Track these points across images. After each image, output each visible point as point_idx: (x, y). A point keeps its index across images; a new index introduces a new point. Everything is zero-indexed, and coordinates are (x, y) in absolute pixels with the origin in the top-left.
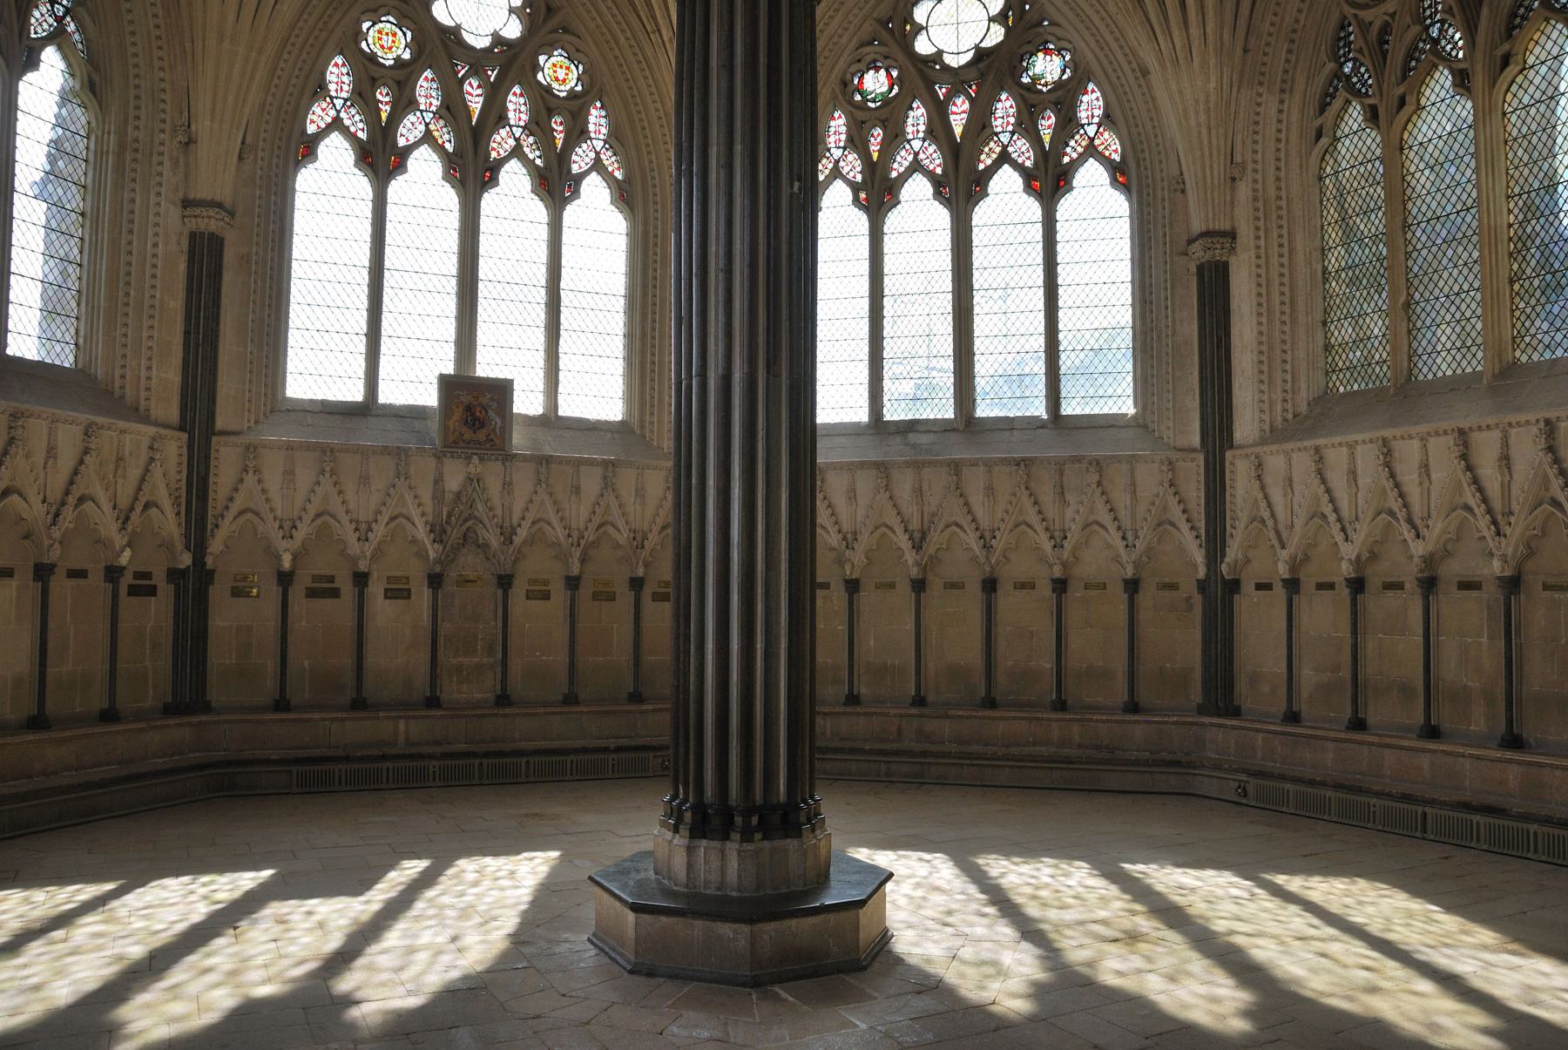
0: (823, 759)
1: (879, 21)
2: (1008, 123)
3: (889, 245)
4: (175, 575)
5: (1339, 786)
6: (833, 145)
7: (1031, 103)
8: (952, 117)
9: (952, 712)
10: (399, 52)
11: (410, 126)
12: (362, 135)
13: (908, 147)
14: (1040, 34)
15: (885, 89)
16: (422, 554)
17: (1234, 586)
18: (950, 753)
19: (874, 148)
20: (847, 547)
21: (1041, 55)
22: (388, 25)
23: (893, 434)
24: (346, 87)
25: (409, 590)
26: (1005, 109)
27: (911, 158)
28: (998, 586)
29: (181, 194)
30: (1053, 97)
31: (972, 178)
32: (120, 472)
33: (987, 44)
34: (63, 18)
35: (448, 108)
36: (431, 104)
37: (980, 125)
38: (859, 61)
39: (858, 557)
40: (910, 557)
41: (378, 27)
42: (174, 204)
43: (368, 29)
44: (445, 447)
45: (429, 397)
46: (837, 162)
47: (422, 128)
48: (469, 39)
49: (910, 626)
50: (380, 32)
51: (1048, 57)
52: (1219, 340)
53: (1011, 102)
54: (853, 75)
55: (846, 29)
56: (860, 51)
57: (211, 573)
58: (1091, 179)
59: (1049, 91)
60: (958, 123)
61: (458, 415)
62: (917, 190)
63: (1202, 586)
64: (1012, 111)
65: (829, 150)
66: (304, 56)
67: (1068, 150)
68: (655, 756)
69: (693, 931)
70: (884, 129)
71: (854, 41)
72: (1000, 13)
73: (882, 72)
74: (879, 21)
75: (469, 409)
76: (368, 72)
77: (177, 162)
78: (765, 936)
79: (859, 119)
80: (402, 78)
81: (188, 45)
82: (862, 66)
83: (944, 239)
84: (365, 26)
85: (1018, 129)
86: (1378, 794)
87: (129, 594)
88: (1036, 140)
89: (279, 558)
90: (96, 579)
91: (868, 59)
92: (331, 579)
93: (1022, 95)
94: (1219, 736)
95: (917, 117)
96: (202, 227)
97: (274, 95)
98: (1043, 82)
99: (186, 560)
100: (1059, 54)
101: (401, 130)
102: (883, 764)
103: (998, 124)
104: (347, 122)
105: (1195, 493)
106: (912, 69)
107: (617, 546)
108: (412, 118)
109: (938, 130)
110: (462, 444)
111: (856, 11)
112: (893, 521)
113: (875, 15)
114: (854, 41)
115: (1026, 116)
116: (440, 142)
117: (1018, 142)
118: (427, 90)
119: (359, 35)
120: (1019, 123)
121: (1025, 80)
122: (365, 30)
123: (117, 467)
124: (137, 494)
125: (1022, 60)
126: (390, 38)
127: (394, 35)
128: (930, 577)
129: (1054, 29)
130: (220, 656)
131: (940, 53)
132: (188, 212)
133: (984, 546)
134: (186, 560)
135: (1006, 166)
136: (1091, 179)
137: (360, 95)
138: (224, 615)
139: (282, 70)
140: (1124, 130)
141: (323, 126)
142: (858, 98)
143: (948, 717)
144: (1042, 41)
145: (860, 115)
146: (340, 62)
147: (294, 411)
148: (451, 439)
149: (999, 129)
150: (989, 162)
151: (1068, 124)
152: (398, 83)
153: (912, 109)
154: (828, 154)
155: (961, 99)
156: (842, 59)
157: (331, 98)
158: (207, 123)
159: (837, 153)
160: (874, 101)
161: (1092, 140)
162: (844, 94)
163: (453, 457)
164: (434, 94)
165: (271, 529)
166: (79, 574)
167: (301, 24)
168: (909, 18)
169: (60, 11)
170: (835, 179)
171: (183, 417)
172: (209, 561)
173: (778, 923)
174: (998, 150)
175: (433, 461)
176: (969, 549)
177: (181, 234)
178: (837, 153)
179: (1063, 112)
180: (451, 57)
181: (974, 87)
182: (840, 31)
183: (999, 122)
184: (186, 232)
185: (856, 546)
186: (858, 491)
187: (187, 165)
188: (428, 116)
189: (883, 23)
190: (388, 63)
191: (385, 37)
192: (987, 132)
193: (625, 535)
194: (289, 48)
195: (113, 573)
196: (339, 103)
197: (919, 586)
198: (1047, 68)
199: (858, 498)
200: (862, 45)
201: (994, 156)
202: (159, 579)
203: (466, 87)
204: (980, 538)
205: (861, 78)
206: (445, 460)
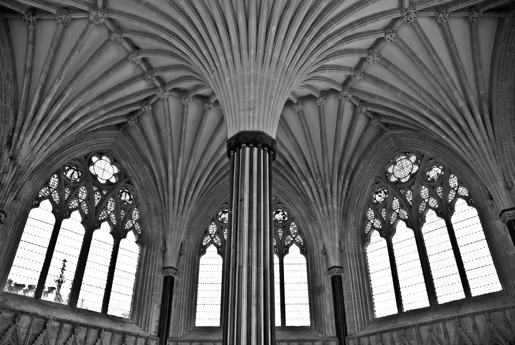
7: (432, 185)
26: (424, 192)
53: (426, 189)
58: (461, 205)
64: (427, 192)
67: (450, 198)
70: (386, 208)
85: (430, 196)
109: (404, 205)
135: (430, 210)
136: (461, 205)
151: (447, 189)
179: (443, 185)
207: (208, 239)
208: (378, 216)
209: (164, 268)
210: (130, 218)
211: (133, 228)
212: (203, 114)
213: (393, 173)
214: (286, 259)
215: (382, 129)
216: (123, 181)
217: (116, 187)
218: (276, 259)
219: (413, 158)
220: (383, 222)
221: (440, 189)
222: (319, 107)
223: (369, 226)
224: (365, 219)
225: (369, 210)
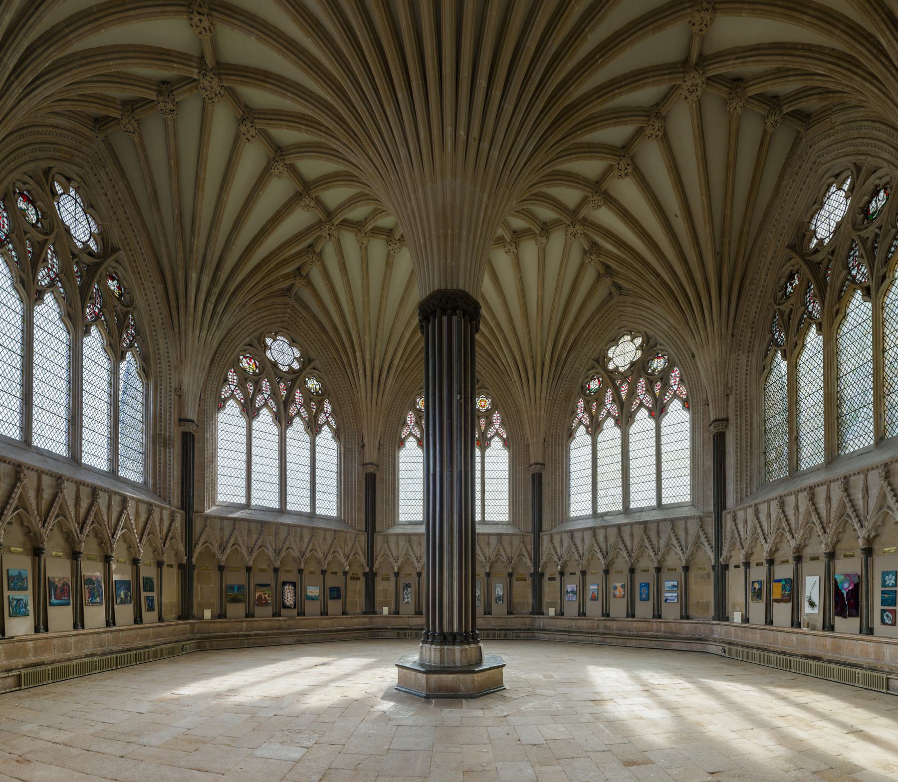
5: (758, 648)
17: (726, 567)
21: (656, 360)
26: (642, 382)
52: (721, 465)
58: (676, 406)
63: (713, 567)
86: (773, 652)
94: (719, 630)
105: (711, 530)
107: (503, 562)
121: (650, 371)
129: (661, 347)
136: (676, 406)
140: (687, 384)
151: (666, 385)
161: (676, 391)
198: (658, 364)
208: (587, 409)
214: (488, 452)
218: (478, 452)
219: (638, 341)
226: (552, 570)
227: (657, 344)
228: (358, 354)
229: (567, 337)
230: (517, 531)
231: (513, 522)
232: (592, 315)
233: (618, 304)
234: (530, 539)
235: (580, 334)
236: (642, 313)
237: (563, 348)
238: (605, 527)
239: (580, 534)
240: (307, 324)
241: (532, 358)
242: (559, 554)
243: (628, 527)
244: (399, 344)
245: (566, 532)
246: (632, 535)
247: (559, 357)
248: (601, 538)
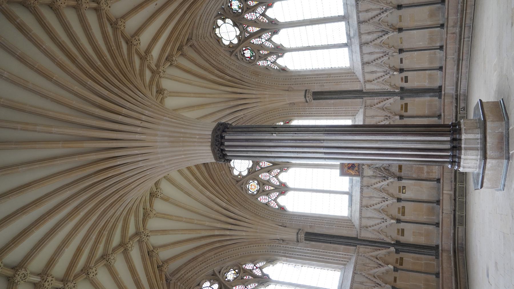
0: (462, 59)
1: (231, 55)
2: (253, 14)
3: (293, 46)
4: (397, 252)
6: (267, 64)
8: (254, 31)
9: (446, 17)
10: (256, 184)
11: (274, 181)
12: (278, 193)
13: (264, 43)
14: (227, 9)
15: (249, 51)
16: (392, 182)
18: (461, 18)
19: (266, 52)
20: (388, 54)
21: (232, 7)
22: (249, 187)
23: (351, 41)
24: (266, 198)
25: (403, 187)
26: (248, 16)
27: (268, 42)
28: (400, 4)
29: (296, 243)
30: (244, 3)
31: (271, 24)
32: (367, 265)
33: (232, 23)
34: (256, 267)
35: (269, 171)
36: (268, 176)
37: (255, 23)
38: (242, 59)
39: (391, 51)
40: (390, 34)
41: (250, 190)
42: (298, 244)
43: (251, 192)
44: (360, 175)
45: (346, 179)
46: (271, 62)
47: (274, 178)
48: (250, 166)
49: (415, 31)
50: (251, 189)
51: (233, 5)
54: (247, 60)
55: (234, 64)
56: (239, 59)
57: (397, 241)
59: (242, 4)
60: (256, 29)
61: (351, 171)
62: (277, 39)
65: (268, 65)
66: (259, 209)
68: (460, 114)
69: (489, 173)
70: (260, 50)
71: (237, 61)
72: (223, 21)
73: (245, 52)
74: (231, 55)
75: (349, 168)
76: (261, 192)
77: (288, 243)
78: (492, 154)
79: (258, 57)
80: (262, 183)
81: (259, 239)
82: (244, 58)
83: (290, 30)
84: (250, 192)
85: (254, 11)
87: (402, 265)
88: (256, 6)
89: (392, 223)
90: (397, 274)
91: (241, 57)
92: (399, 209)
93: (245, 12)
95: (255, 41)
96: (303, 238)
97: (269, 218)
98: (240, 6)
99: (392, 249)
100: (231, 2)
101: (275, 183)
102: (465, 40)
103: (254, 18)
104: (275, 198)
106: (243, 44)
108: (272, 181)
109: (258, 35)
110: (359, 170)
111: (229, 62)
112: (378, 41)
113: (229, 56)
114: (237, 61)
115: (251, 10)
116: (277, 173)
117: (258, 11)
118: (264, 176)
119: (253, 195)
120: (253, 11)
121: (240, 11)
122: (251, 193)
123: (366, 266)
124: (373, 261)
125: (235, 13)
126: (252, 186)
127: (251, 185)
128: (397, 27)
129: (225, 4)
130: (422, 241)
131: (237, 36)
132: (300, 241)
133: (386, 11)
134: (392, 249)
137: (267, 194)
138: (409, 238)
139: (263, 215)
141: (276, 204)
142: (252, 58)
143: (448, 18)
144: (229, 8)
145: (257, 57)
146: (260, 199)
147: (351, 215)
148: (358, 173)
149: (256, 17)
150: (265, 19)
152: (263, 184)
153: (253, 43)
154: (270, 65)
155: (249, 29)
156: (243, 64)
157: (269, 201)
158: (277, 236)
159: (269, 63)
160: (253, 54)
162: (252, 62)
163: (363, 173)
164: (265, 175)
165: (383, 225)
166: (395, 280)
167: (251, 210)
168: (229, 46)
169: (255, 268)
170: (276, 63)
171: (353, 246)
172: (393, 242)
173: (487, 150)
174: (262, 17)
175: (364, 178)
176: (387, 16)
177: (305, 243)
178: (269, 63)
180: (256, 171)
181: (245, 26)
182: (235, 66)
183: (253, 17)
184: (305, 241)
185: (387, 52)
186: (370, 52)
187: (288, 241)
188: (271, 176)
189: (231, 53)
190: (259, 187)
191: (252, 188)
192: (257, 21)
193: (386, 122)
194: (257, 213)
195: (396, 270)
196: (270, 200)
197: (400, 30)
199: (372, 52)
200: (238, 59)
201: (263, 18)
202: (398, 256)
203: (263, 166)
204: (383, 13)
205: (247, 57)
206: (364, 175)
207: (273, 204)
209: (298, 241)
210: (252, 270)
211: (261, 268)
212: (166, 199)
213: (230, 41)
215: (191, 46)
216: (219, 278)
217: (224, 284)
219: (220, 22)
220: (270, 54)
221: (250, 2)
222: (169, 96)
223: (273, 66)
224: (267, 68)
225: (259, 64)
226: (397, 79)
227: (222, 7)
228: (217, 233)
229: (217, 76)
230: (362, 111)
231: (353, 115)
232: (203, 58)
233: (197, 40)
234: (369, 101)
235: (214, 67)
236: (203, 21)
237: (223, 78)
238: (360, 34)
239: (365, 56)
240: (190, 271)
241: (229, 101)
242: (383, 74)
243: (360, 14)
244: (213, 201)
245: (363, 69)
246: (367, 11)
247: (229, 81)
248: (370, 38)
